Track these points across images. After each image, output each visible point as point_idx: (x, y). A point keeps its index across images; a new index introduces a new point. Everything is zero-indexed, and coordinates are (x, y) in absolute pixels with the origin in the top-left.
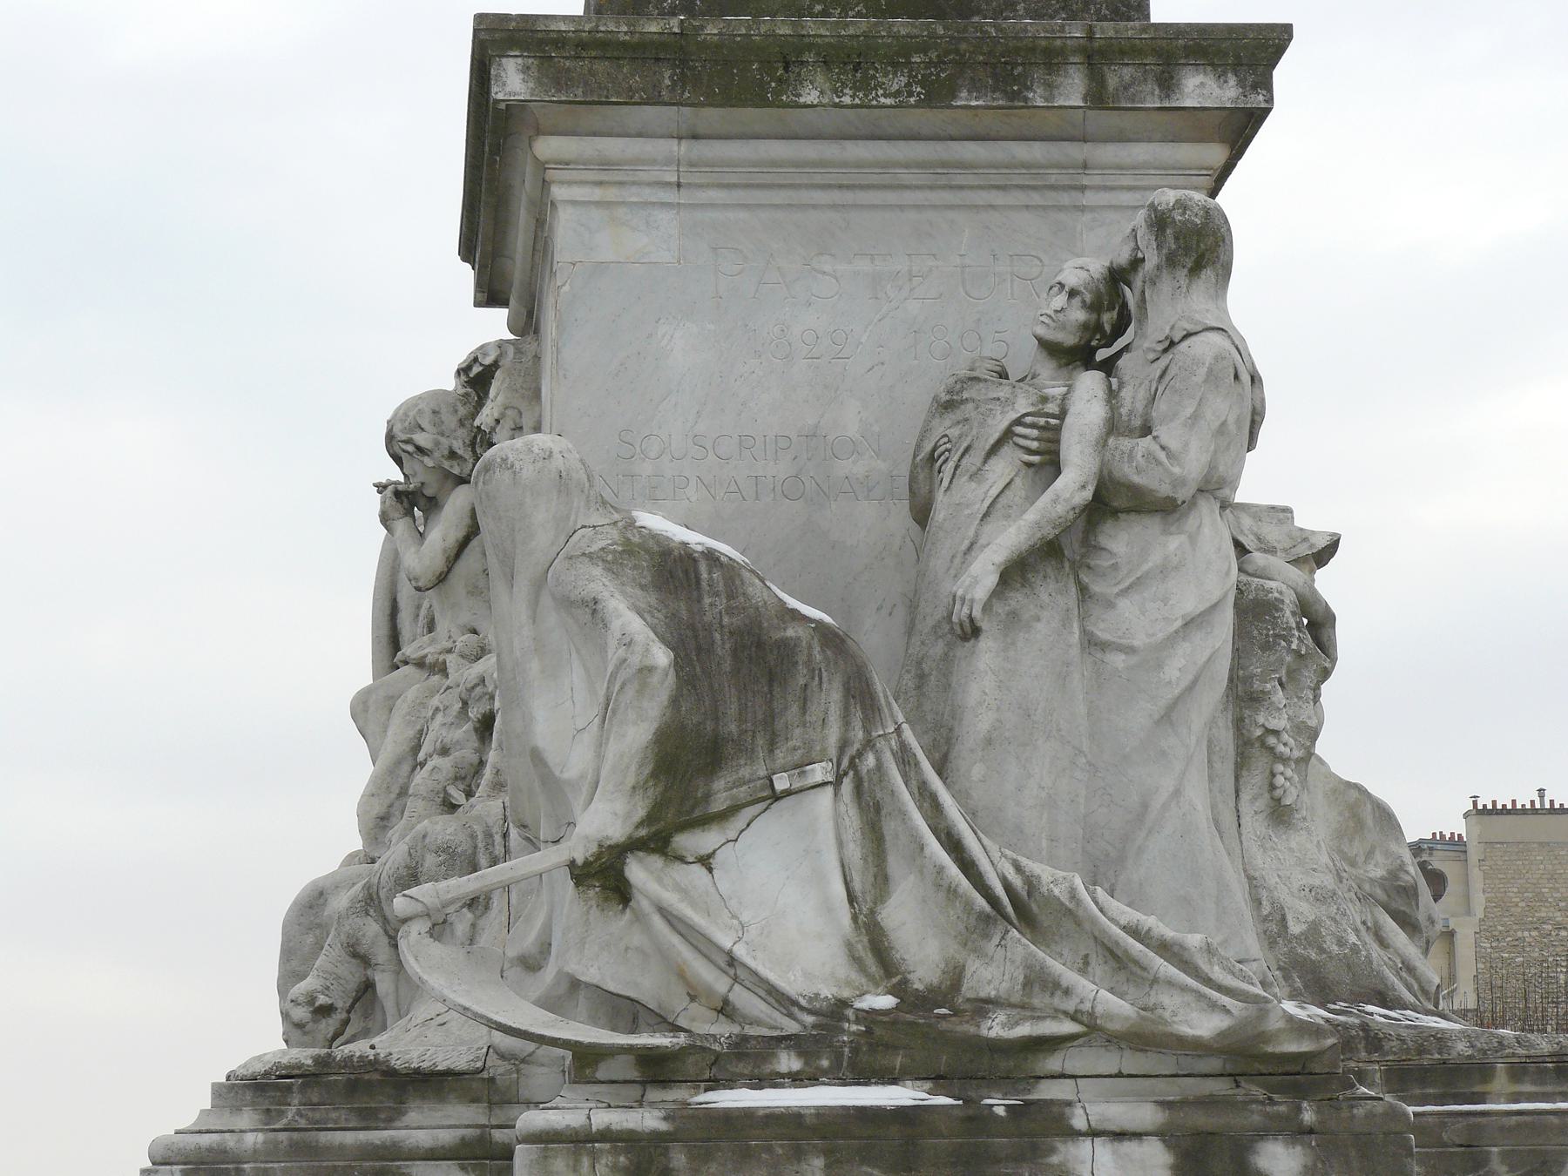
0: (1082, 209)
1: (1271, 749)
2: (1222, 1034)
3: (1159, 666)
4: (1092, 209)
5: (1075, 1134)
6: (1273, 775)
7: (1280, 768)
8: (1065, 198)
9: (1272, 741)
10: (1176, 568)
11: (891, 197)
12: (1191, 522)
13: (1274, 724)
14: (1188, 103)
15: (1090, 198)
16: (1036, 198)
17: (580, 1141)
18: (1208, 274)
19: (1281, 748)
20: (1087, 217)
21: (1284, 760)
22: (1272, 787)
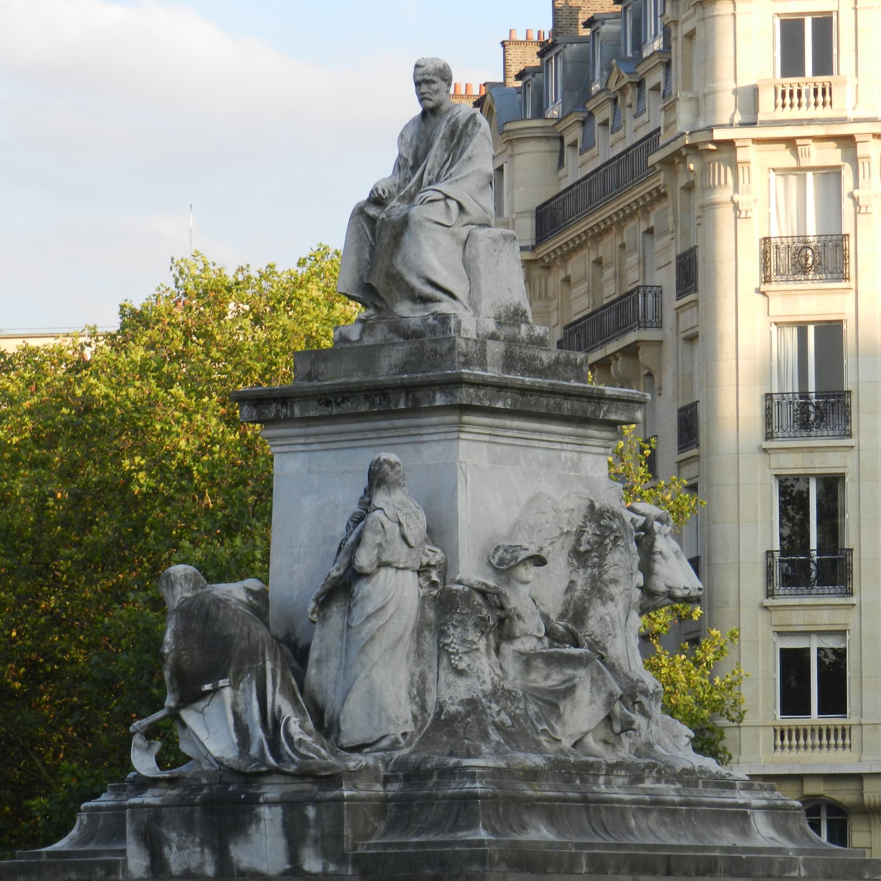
0: (424, 442)
1: (447, 651)
2: (296, 770)
3: (360, 633)
4: (426, 442)
5: (259, 804)
6: (451, 660)
7: (452, 657)
8: (417, 439)
9: (446, 648)
10: (367, 597)
11: (367, 443)
12: (374, 579)
13: (448, 641)
14: (437, 404)
15: (424, 438)
16: (408, 439)
17: (142, 806)
18: (383, 487)
19: (451, 650)
20: (425, 445)
21: (457, 654)
22: (452, 665)
